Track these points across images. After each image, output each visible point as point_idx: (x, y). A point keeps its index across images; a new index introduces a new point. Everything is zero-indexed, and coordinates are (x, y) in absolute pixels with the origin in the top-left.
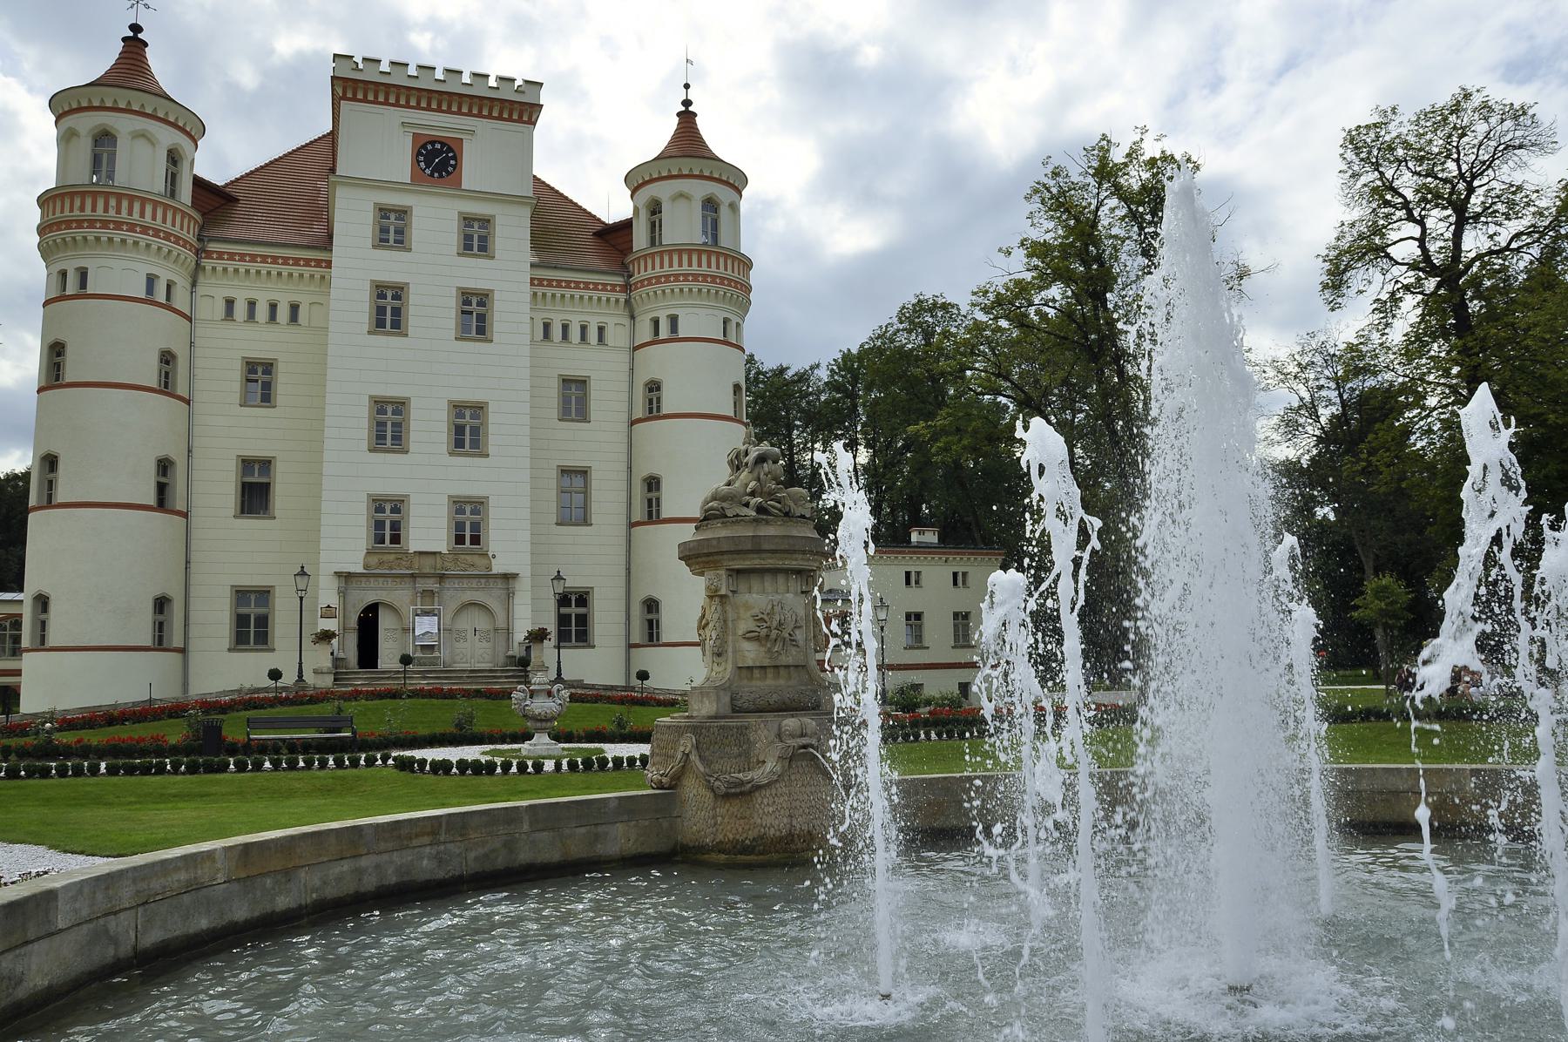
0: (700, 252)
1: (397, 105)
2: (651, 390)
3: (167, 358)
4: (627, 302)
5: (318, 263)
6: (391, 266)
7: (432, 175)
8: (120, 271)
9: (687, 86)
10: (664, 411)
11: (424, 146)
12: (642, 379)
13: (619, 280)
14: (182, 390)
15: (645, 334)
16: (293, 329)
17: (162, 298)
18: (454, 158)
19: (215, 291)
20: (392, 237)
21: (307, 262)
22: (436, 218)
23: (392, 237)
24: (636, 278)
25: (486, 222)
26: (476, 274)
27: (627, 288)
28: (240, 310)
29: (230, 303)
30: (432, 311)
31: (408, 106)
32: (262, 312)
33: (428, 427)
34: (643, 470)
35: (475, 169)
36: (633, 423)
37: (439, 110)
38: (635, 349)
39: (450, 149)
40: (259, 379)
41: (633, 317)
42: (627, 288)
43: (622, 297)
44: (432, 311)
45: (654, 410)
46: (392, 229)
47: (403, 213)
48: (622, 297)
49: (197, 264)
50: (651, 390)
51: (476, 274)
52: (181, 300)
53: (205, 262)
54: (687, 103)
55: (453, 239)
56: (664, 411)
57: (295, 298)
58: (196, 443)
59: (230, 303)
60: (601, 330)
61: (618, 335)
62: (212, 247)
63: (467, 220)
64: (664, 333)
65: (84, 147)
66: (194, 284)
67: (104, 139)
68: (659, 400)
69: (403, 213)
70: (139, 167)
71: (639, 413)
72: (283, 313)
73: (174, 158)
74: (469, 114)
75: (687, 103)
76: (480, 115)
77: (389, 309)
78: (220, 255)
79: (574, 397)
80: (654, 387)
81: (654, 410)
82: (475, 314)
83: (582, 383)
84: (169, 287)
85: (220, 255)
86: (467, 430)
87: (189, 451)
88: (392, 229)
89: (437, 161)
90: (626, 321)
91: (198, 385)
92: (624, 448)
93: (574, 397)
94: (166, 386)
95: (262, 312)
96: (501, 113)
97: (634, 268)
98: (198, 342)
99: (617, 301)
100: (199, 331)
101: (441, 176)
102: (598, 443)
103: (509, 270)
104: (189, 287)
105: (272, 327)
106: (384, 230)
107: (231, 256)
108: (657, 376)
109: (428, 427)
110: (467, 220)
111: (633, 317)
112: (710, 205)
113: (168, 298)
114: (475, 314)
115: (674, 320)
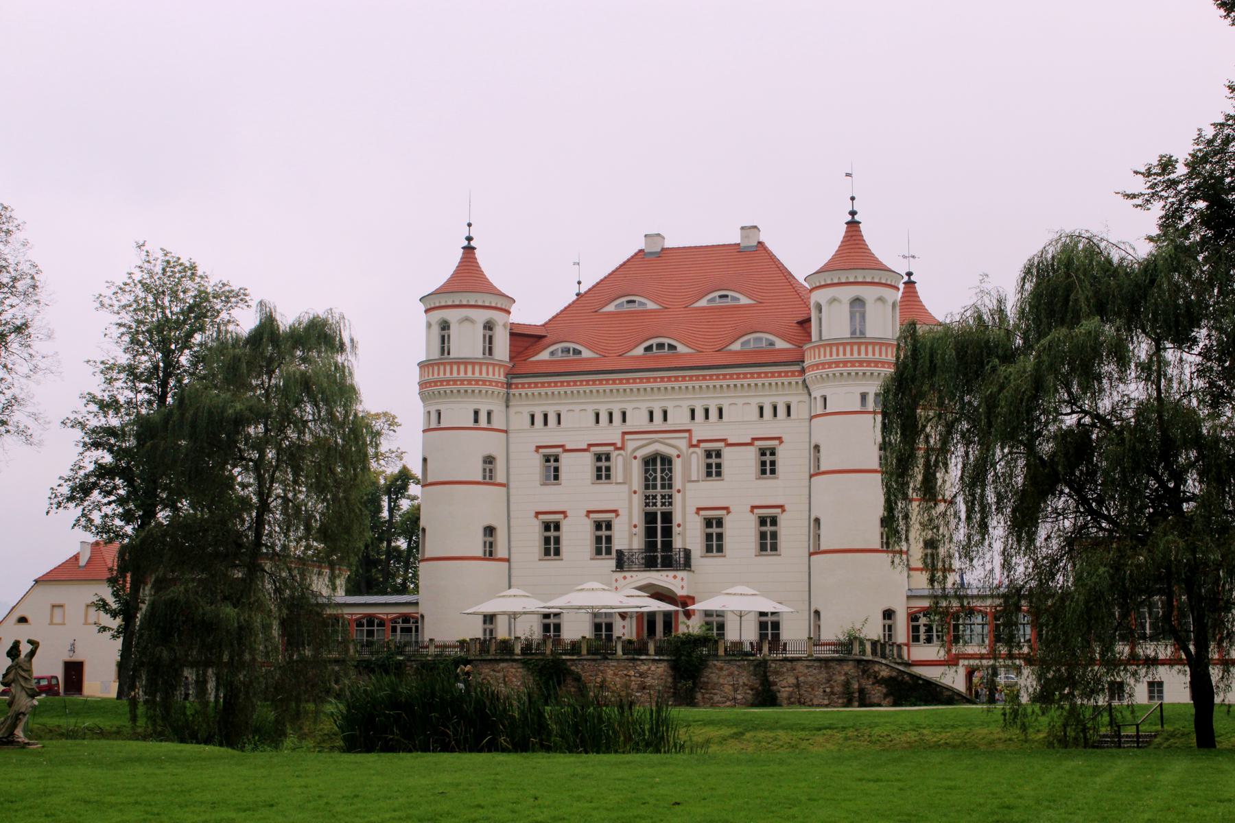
0: (844, 344)
8: (458, 412)
13: (797, 368)
24: (806, 364)
34: (813, 518)
36: (811, 476)
38: (812, 418)
42: (803, 371)
43: (800, 380)
48: (800, 380)
52: (498, 422)
61: (800, 411)
65: (436, 330)
66: (507, 406)
67: (445, 326)
70: (467, 343)
73: (489, 326)
84: (489, 414)
97: (807, 355)
104: (504, 408)
112: (858, 302)
113: (489, 421)
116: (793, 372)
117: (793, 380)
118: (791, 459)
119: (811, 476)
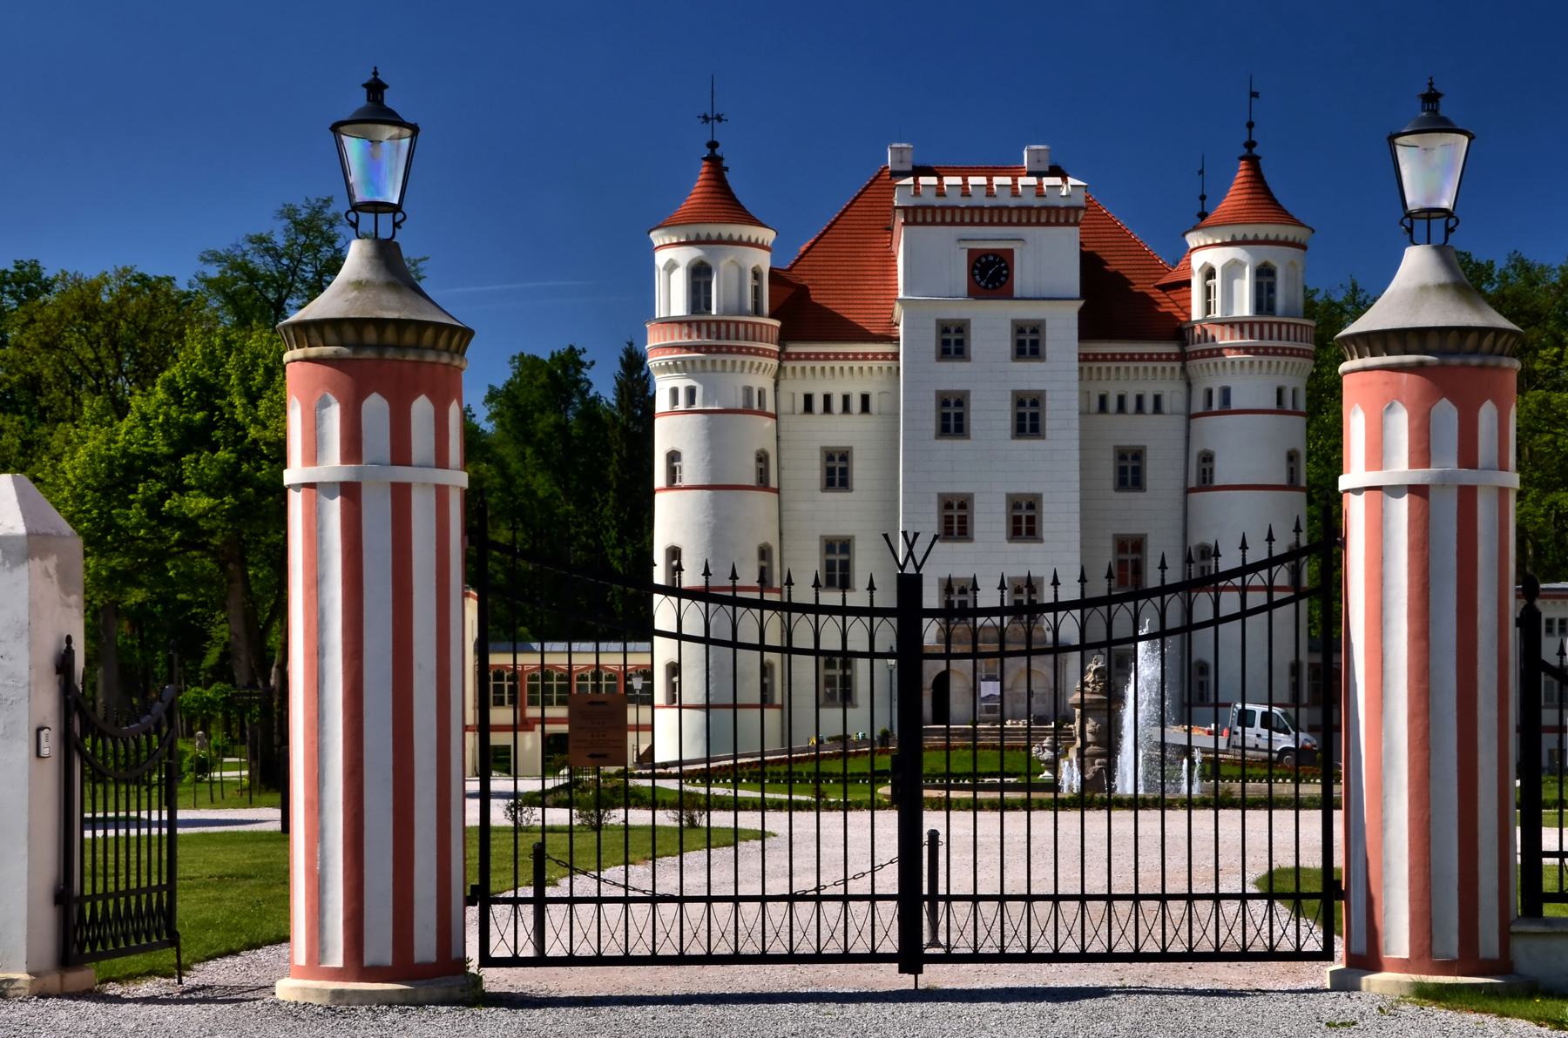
1: (953, 223)
2: (1205, 460)
3: (762, 458)
4: (1183, 369)
5: (885, 356)
6: (953, 376)
7: (986, 287)
9: (1250, 125)
10: (1217, 482)
11: (978, 260)
12: (1195, 450)
13: (1172, 348)
14: (773, 483)
15: (1198, 406)
16: (865, 417)
17: (756, 407)
18: (1006, 268)
19: (796, 387)
20: (953, 347)
21: (875, 356)
22: (991, 323)
23: (953, 347)
25: (1037, 328)
26: (1029, 375)
27: (1183, 357)
28: (818, 404)
29: (808, 399)
30: (991, 416)
31: (962, 223)
32: (837, 404)
33: (990, 519)
34: (1196, 540)
35: (1022, 277)
36: (1188, 491)
37: (991, 223)
38: (1190, 416)
39: (1002, 260)
40: (837, 471)
41: (1189, 385)
42: (1183, 357)
43: (1177, 365)
44: (991, 416)
45: (1206, 482)
46: (953, 342)
47: (962, 328)
49: (780, 366)
50: (1205, 460)
51: (1029, 375)
53: (788, 365)
54: (1250, 145)
55: (1007, 345)
56: (1217, 482)
57: (866, 389)
58: (785, 525)
59: (808, 399)
60: (1157, 399)
62: (793, 348)
63: (1019, 328)
64: (1215, 407)
66: (776, 385)
68: (1211, 470)
69: (962, 328)
71: (1193, 483)
72: (856, 404)
74: (1019, 224)
75: (1250, 145)
76: (1029, 224)
77: (952, 418)
78: (798, 357)
79: (1130, 471)
80: (1207, 458)
81: (1206, 482)
82: (1028, 418)
83: (1138, 455)
85: (798, 357)
86: (1024, 521)
87: (781, 534)
88: (953, 342)
89: (991, 276)
90: (1182, 387)
91: (784, 474)
92: (1179, 514)
93: (1130, 471)
94: (763, 483)
95: (837, 404)
96: (1048, 218)
98: (783, 435)
99: (1173, 369)
100: (783, 426)
101: (995, 287)
102: (1152, 514)
103: (1059, 374)
105: (846, 417)
106: (945, 343)
107: (808, 356)
108: (1210, 448)
109: (990, 519)
110: (1019, 328)
111: (1189, 385)
114: (1028, 418)
115: (1226, 393)
116: (1169, 355)
117: (1168, 365)
118: (1163, 472)
119: (1188, 491)
